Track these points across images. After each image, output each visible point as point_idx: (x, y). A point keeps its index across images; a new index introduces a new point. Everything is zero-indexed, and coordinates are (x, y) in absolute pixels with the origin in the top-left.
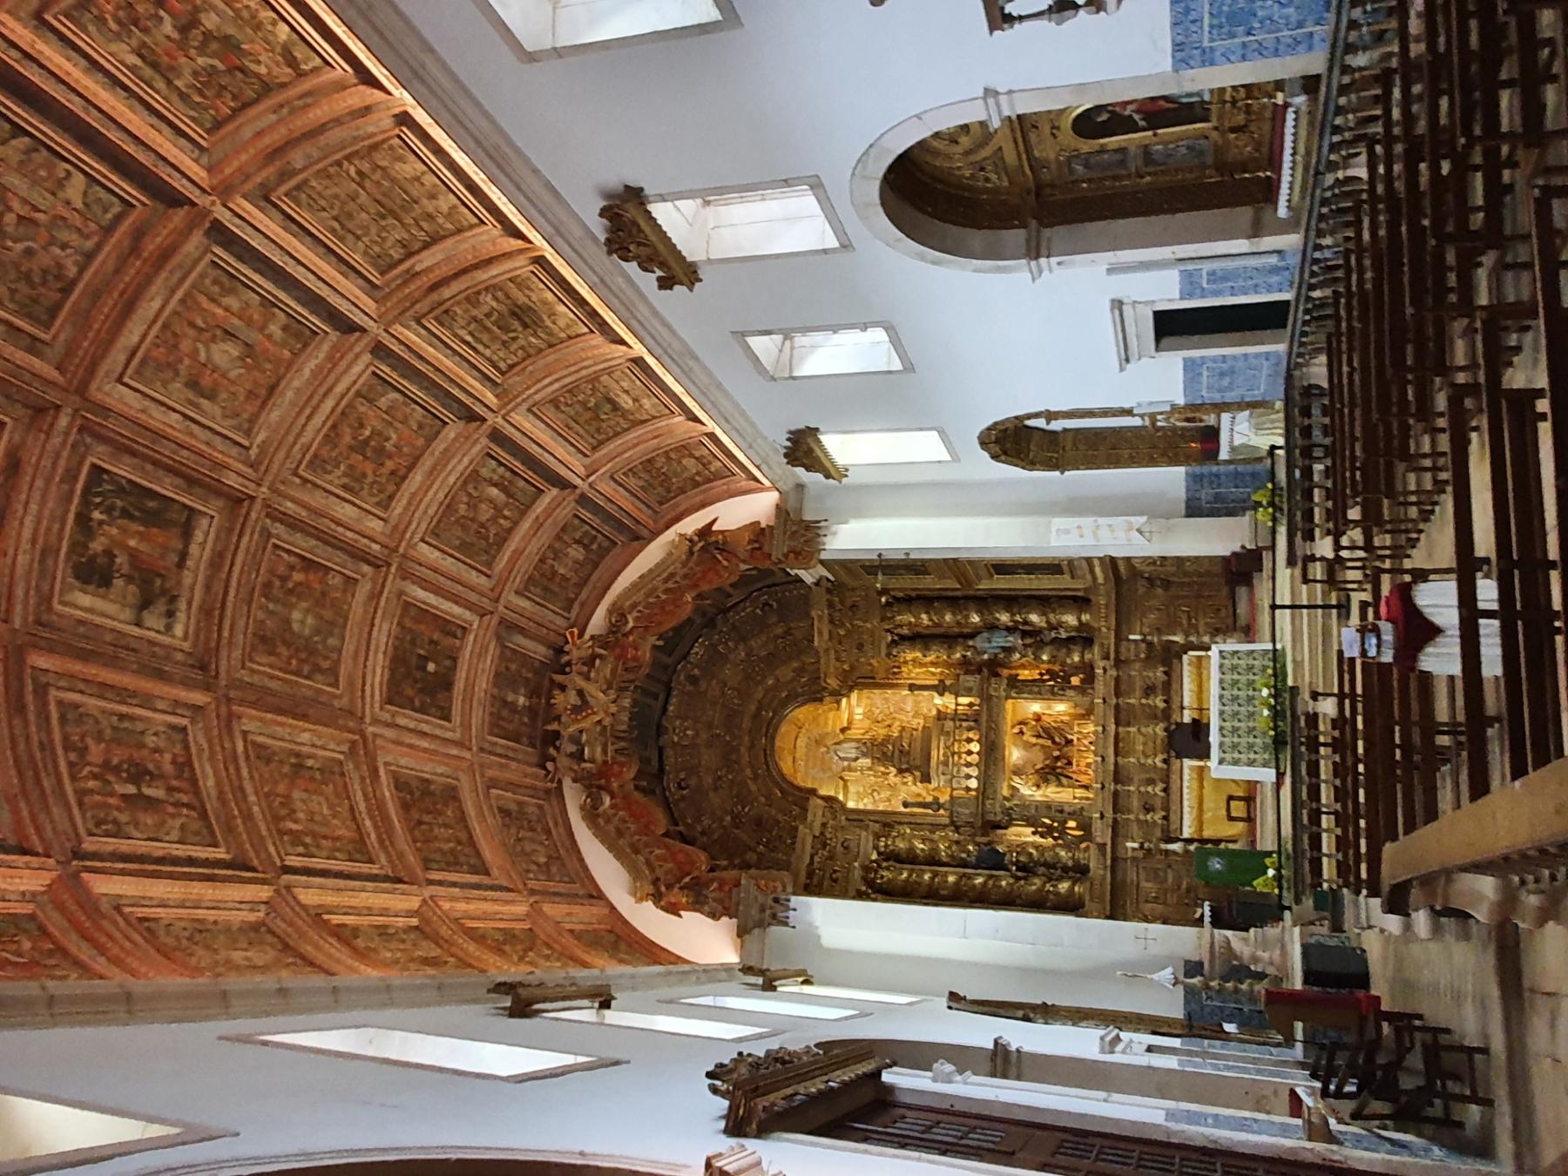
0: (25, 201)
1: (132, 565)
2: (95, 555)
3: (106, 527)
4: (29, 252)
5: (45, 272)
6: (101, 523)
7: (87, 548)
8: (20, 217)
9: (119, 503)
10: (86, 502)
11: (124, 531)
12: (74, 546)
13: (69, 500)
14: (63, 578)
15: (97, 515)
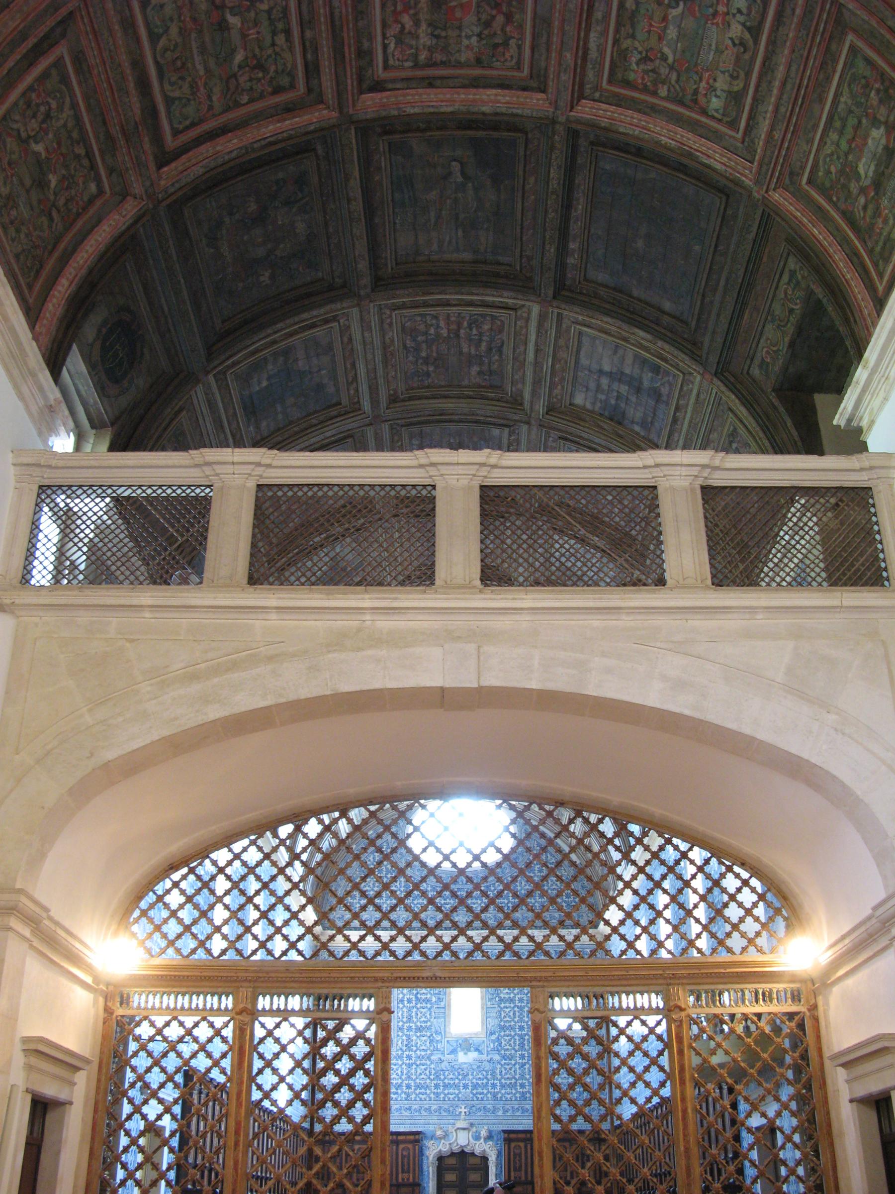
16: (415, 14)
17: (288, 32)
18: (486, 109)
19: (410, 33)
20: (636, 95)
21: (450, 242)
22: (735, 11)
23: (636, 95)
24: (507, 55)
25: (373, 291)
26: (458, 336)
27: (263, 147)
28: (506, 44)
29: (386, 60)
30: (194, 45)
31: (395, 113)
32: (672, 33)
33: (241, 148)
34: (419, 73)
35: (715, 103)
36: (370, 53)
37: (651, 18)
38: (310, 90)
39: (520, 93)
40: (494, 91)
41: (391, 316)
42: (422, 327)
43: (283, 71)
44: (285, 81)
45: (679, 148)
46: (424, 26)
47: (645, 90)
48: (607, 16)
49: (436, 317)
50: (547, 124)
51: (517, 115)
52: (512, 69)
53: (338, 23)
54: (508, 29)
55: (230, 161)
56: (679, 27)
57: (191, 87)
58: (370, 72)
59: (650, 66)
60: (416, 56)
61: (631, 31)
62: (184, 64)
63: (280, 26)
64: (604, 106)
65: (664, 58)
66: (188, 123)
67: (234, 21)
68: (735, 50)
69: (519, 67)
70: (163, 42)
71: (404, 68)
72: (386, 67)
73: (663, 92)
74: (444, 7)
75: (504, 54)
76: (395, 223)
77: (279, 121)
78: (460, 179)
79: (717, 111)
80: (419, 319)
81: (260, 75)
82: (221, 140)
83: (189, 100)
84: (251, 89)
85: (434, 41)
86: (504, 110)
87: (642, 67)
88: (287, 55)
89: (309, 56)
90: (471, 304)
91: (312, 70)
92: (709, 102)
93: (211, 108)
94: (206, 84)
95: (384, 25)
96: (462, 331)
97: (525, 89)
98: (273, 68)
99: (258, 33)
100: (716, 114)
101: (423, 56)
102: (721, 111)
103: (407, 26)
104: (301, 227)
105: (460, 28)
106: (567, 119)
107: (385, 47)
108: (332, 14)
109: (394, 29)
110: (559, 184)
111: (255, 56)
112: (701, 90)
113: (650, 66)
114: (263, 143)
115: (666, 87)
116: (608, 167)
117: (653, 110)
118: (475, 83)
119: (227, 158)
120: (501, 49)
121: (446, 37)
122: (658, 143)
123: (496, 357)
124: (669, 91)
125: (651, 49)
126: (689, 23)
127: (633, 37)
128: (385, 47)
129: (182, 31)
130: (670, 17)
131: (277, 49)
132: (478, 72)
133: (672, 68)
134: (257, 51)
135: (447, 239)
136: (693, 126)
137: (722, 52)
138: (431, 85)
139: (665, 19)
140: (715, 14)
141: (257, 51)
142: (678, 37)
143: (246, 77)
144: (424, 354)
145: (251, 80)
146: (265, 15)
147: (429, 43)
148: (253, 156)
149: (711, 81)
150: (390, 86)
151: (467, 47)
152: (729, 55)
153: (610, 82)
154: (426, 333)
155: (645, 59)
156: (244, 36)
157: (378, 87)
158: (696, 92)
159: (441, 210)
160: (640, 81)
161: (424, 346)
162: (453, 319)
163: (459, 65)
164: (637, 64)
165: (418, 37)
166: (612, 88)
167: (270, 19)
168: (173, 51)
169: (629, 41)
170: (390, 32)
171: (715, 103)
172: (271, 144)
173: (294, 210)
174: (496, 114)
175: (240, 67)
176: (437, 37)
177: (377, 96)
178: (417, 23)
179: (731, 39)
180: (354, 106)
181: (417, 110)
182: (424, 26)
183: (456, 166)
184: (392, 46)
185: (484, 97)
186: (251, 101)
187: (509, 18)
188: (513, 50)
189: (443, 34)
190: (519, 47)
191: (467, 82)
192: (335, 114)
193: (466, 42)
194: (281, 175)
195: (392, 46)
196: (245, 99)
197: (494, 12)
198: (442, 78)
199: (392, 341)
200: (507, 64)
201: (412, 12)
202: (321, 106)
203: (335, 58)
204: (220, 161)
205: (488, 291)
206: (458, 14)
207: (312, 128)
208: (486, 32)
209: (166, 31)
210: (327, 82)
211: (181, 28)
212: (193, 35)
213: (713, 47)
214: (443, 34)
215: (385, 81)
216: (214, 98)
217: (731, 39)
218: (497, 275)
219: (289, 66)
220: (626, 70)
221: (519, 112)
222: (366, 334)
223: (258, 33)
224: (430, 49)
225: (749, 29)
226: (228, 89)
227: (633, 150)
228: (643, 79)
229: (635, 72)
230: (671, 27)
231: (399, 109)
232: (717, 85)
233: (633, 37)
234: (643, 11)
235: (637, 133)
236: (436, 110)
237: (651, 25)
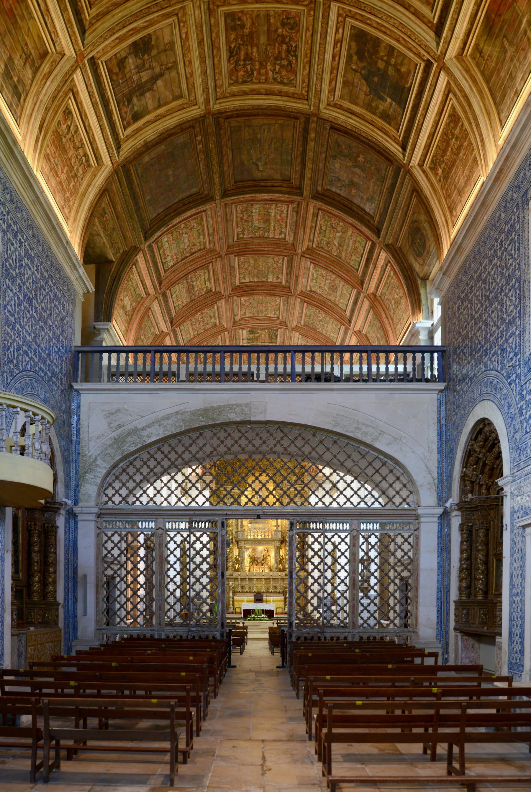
21: (264, 131)
26: (261, 64)
28: (242, 212)
36: (293, 211)
41: (302, 88)
42: (284, 73)
46: (272, 215)
78: (259, 163)
80: (285, 81)
95: (287, 217)
96: (257, 67)
107: (288, 211)
123: (233, 46)
128: (288, 211)
144: (285, 47)
154: (282, 66)
159: (269, 149)
161: (283, 55)
182: (272, 215)
183: (261, 168)
184: (285, 211)
187: (241, 219)
188: (239, 210)
190: (237, 211)
195: (285, 211)
199: (304, 67)
222: (319, 88)
224: (270, 208)
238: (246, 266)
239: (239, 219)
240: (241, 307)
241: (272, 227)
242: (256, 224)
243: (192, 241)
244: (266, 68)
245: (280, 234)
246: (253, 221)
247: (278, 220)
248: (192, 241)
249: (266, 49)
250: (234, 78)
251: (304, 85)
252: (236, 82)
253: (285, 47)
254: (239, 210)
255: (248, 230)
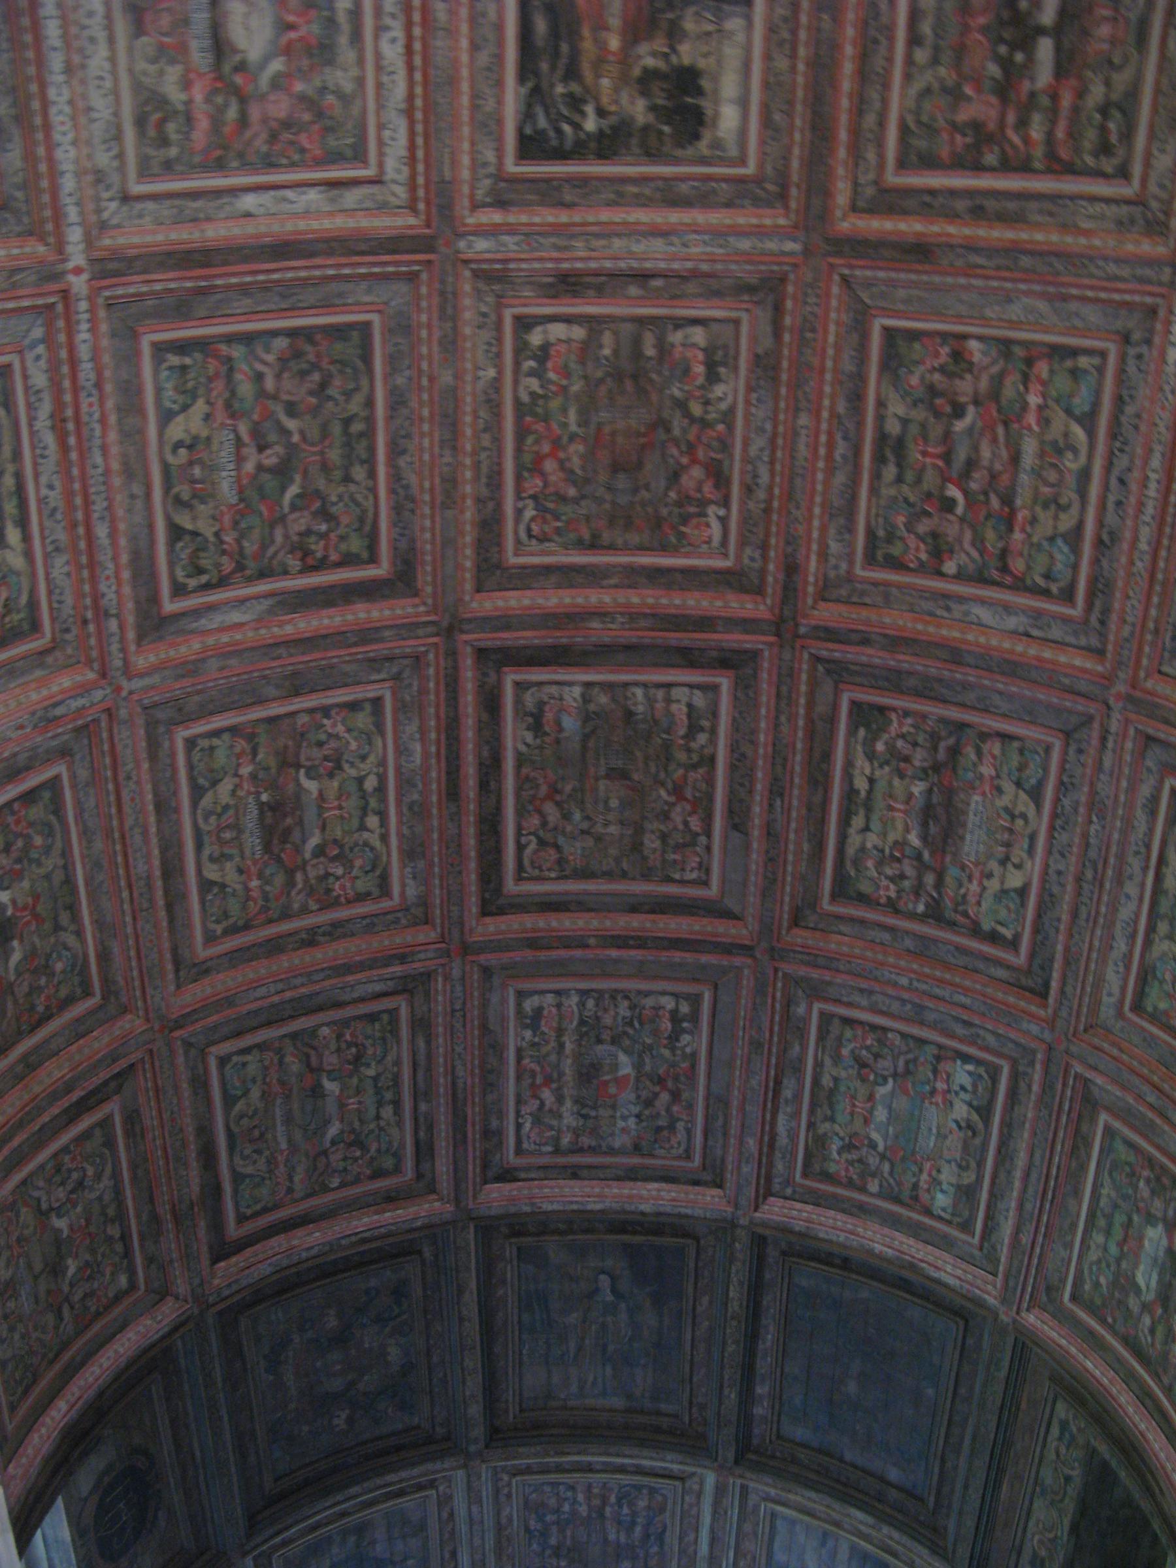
0: (240, 459)
1: (650, 37)
2: (653, 108)
3: (605, 100)
4: (292, 410)
5: (303, 374)
6: (601, 113)
7: (646, 129)
8: (261, 449)
9: (560, 89)
10: (578, 151)
11: (599, 63)
12: (651, 154)
13: (583, 182)
14: (703, 161)
15: (591, 124)
16: (559, 1089)
17: (397, 1104)
18: (646, 1207)
19: (551, 1111)
20: (839, 1191)
21: (594, 1383)
22: (957, 1088)
23: (839, 1191)
24: (674, 1141)
25: (487, 1447)
26: (602, 1516)
27: (353, 1245)
28: (672, 1127)
29: (519, 1142)
30: (278, 1113)
31: (527, 1209)
32: (881, 1114)
33: (323, 1244)
34: (561, 1160)
35: (942, 1201)
36: (500, 1133)
37: (853, 1097)
38: (419, 1176)
39: (690, 1188)
40: (656, 1185)
41: (509, 1484)
42: (553, 1502)
43: (388, 1150)
44: (388, 1163)
45: (898, 1258)
46: (568, 1104)
47: (850, 1184)
48: (798, 1097)
49: (572, 1488)
50: (724, 1228)
51: (687, 1216)
52: (679, 1158)
53: (460, 1096)
54: (675, 1108)
55: (307, 1260)
56: (890, 1108)
57: (269, 1162)
58: (498, 1156)
59: (854, 1156)
60: (557, 1140)
61: (829, 1113)
62: (262, 1135)
63: (388, 1096)
64: (799, 1205)
65: (873, 1145)
66: (258, 1207)
67: (331, 1087)
68: (961, 1134)
69: (688, 1156)
70: (239, 1106)
71: (541, 1154)
72: (519, 1151)
73: (874, 1187)
74: (595, 1081)
75: (669, 1140)
76: (521, 1354)
77: (377, 1213)
78: (610, 1298)
79: (944, 1210)
81: (358, 1153)
82: (300, 1232)
83: (263, 1179)
84: (345, 1170)
85: (581, 1122)
86: (668, 1210)
87: (845, 1156)
88: (395, 1131)
89: (422, 1134)
90: (622, 1470)
91: (424, 1151)
92: (933, 1198)
93: (290, 1190)
94: (287, 1160)
95: (519, 1101)
96: (608, 1510)
97: (696, 1183)
98: (374, 1147)
99: (360, 1103)
100: (943, 1214)
101: (566, 1140)
102: (950, 1210)
103: (548, 1103)
104: (394, 1353)
105: (614, 1107)
106: (751, 1222)
107: (519, 1127)
108: (454, 1084)
109: (534, 1105)
110: (741, 1306)
111: (353, 1131)
112: (922, 1184)
113: (854, 1156)
114: (353, 1239)
115: (876, 1182)
116: (804, 1283)
117: (862, 1210)
118: (632, 1175)
119: (304, 1255)
120: (665, 1133)
121: (596, 1118)
122: (870, 1252)
123: (655, 1549)
124: (881, 1186)
125: (856, 1134)
126: (902, 1104)
127: (832, 1119)
128: (519, 1127)
129: (264, 1095)
130: (877, 1096)
131: (382, 1123)
132: (636, 1160)
133: (883, 1157)
134: (357, 1124)
135: (591, 1379)
136: (916, 1231)
137: (945, 1137)
138: (575, 1176)
139: (871, 1098)
140: (933, 1092)
141: (357, 1124)
142: (888, 1119)
143: (339, 1155)
144: (553, 1541)
145: (345, 1159)
146: (369, 1082)
147: (574, 1124)
148: (340, 1255)
149: (934, 1173)
150: (523, 1175)
151: (623, 1130)
152: (954, 1142)
153: (805, 1175)
154: (557, 1511)
155: (848, 1147)
156: (342, 1106)
157: (507, 1175)
158: (915, 1186)
159: (583, 1339)
160: (843, 1173)
161: (554, 1529)
162: (596, 1491)
163: (611, 1151)
164: (839, 1154)
165: (560, 1117)
166: (808, 1183)
167: (376, 1086)
168: (251, 1118)
169: (827, 1125)
170: (525, 1110)
171: (942, 1201)
172: (364, 1241)
173: (387, 1329)
174: (659, 1214)
175: (333, 1143)
176: (585, 1117)
177: (506, 1188)
178: (560, 1099)
179: (956, 1122)
180: (475, 1197)
181: (555, 1207)
182: (568, 1104)
184: (528, 1125)
185: (644, 1192)
186: (343, 1185)
187: (676, 1096)
188: (681, 1135)
189: (593, 1113)
190: (689, 1132)
191: (621, 1173)
192: (450, 1208)
193: (621, 1124)
194: (373, 1283)
195: (528, 1125)
196: (335, 1182)
197: (657, 1089)
198: (590, 1167)
199: (510, 1520)
200: (674, 1151)
201: (554, 1086)
202: (435, 1197)
203: (454, 1138)
204: (295, 1259)
205: (645, 1453)
206: (612, 1090)
207: (419, 1223)
208: (647, 1112)
209: (246, 1093)
210: (442, 1167)
211: (264, 1093)
212: (279, 1101)
213: (934, 1131)
214: (593, 1113)
215: (515, 1169)
216: (297, 1179)
217: (956, 1122)
218: (658, 1430)
219: (396, 1144)
220: (825, 1160)
221: (689, 1211)
222: (475, 1509)
223: (360, 1103)
224: (576, 1133)
225: (978, 1110)
226: (315, 1169)
227: (837, 1261)
228: (847, 1170)
229: (838, 1162)
230: (880, 1108)
231: (533, 1204)
232: (943, 1177)
233: (832, 1119)
234: (843, 1089)
235: (841, 1239)
236: (581, 1207)
237: (854, 1105)
238: (677, 816)
239: (685, 1095)
240: (725, 445)
241: (569, 1047)
242: (626, 1066)
243: (862, 1092)
244: (589, 1506)
245: (538, 1012)
246: (637, 1080)
247: (548, 1081)
248: (862, 1092)
249: (589, 1535)
250: (660, 1498)
251: (506, 1491)
252: (652, 1491)
253: (553, 1541)
254: (681, 1135)
255: (656, 1033)
